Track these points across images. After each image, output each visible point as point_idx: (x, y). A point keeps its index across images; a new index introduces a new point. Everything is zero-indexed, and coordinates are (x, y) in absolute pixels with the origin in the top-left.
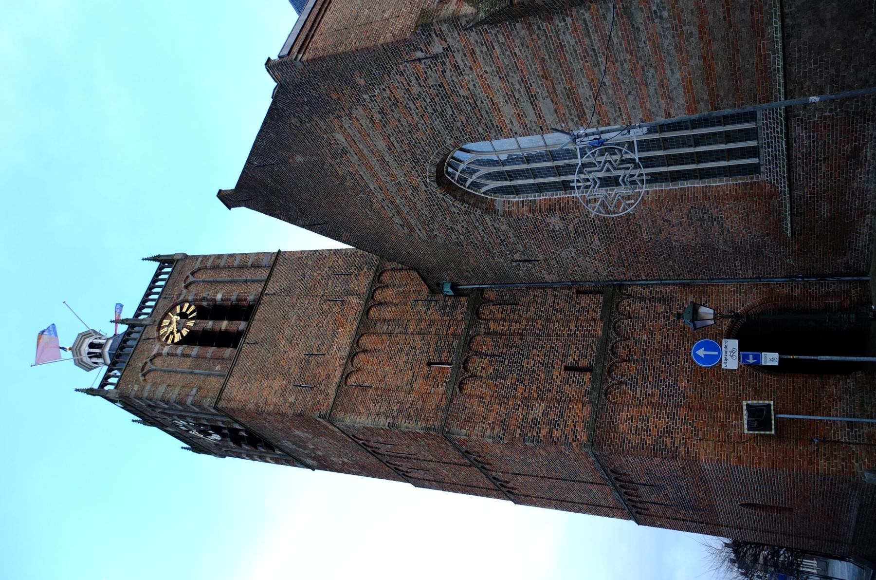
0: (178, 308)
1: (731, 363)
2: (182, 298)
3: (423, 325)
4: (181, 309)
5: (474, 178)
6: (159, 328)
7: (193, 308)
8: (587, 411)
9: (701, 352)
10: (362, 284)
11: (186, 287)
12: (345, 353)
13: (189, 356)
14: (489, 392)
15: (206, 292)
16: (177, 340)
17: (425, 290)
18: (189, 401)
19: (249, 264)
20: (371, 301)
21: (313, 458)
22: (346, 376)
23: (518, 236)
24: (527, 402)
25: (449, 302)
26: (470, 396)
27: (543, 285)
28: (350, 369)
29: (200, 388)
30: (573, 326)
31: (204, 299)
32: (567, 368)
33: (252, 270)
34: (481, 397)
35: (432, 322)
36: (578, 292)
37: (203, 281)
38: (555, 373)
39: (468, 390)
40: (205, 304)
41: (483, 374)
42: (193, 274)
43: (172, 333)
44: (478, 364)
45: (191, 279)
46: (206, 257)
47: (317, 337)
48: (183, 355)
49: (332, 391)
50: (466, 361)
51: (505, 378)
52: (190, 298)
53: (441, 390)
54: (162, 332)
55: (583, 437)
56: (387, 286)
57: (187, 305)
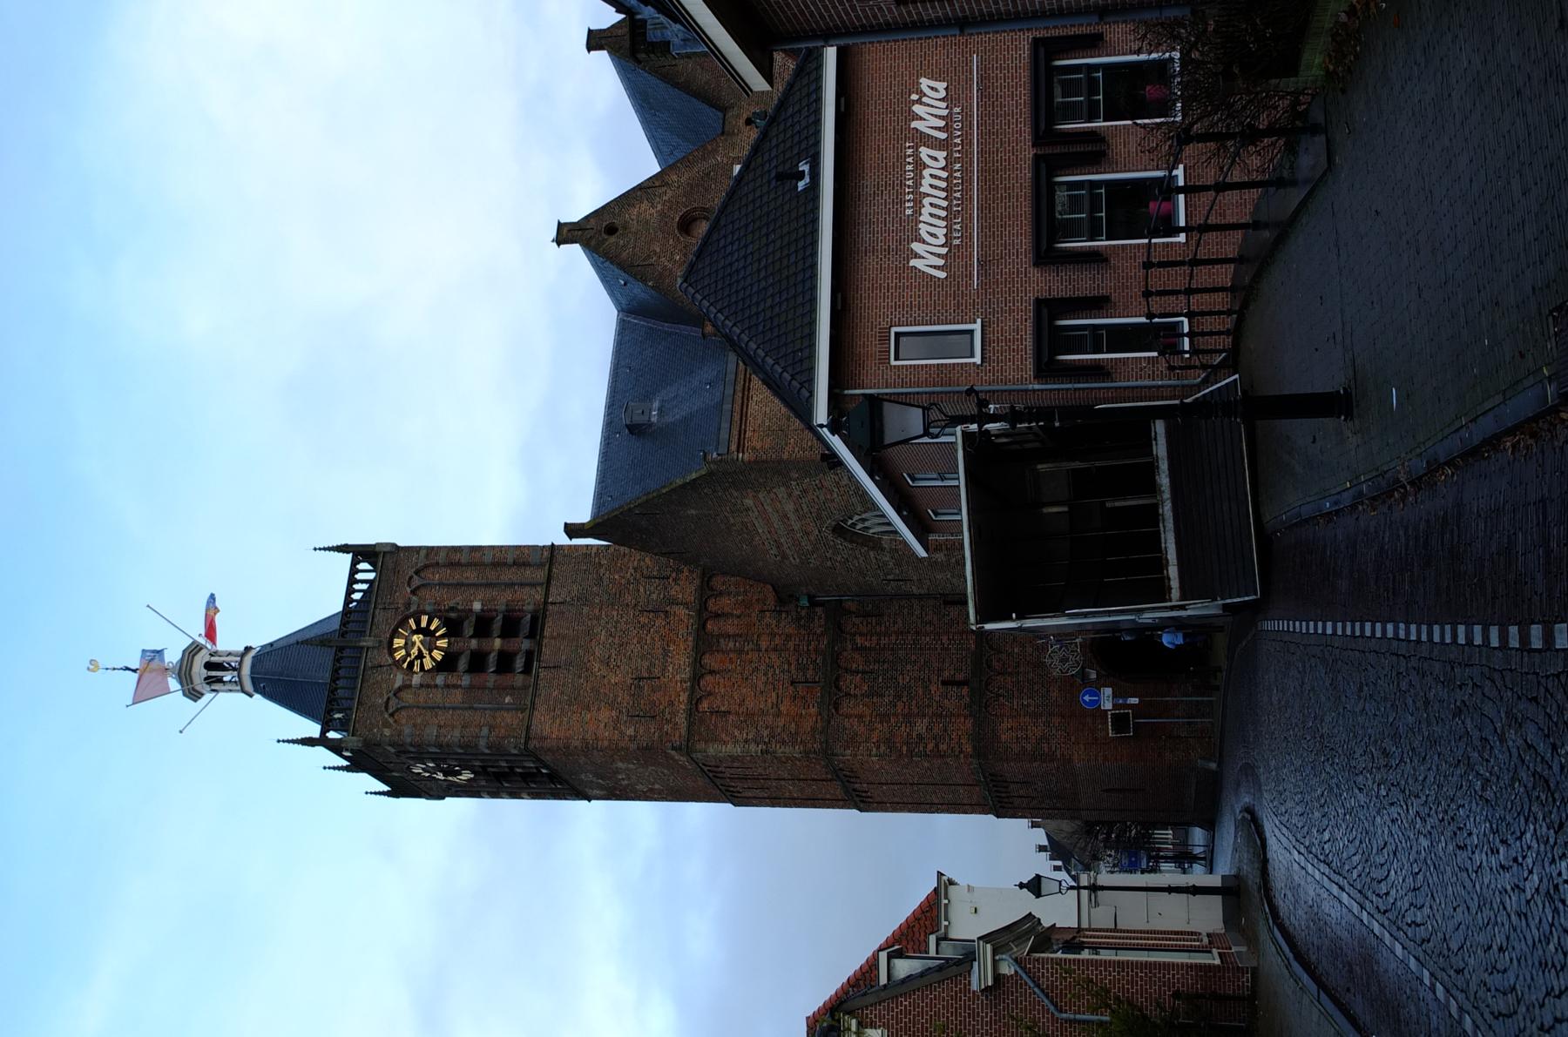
0: (412, 621)
1: (1108, 705)
2: (413, 608)
3: (777, 640)
4: (418, 623)
5: (867, 524)
6: (392, 651)
7: (436, 623)
8: (969, 723)
9: (1087, 698)
10: (685, 588)
11: (413, 592)
12: (686, 673)
13: (456, 687)
14: (868, 712)
15: (457, 600)
16: (428, 664)
17: (771, 601)
18: (482, 743)
19: (510, 560)
20: (703, 613)
21: (601, 787)
22: (694, 702)
23: (898, 564)
24: (909, 718)
25: (803, 613)
26: (848, 716)
27: (909, 596)
28: (698, 694)
29: (491, 728)
30: (945, 639)
31: (452, 609)
32: (944, 683)
33: (513, 569)
34: (860, 717)
35: (789, 637)
36: (947, 603)
37: (441, 584)
38: (933, 688)
39: (844, 709)
40: (453, 615)
41: (858, 692)
42: (417, 573)
43: (420, 656)
44: (851, 682)
45: (416, 582)
46: (431, 550)
47: (643, 657)
48: (447, 686)
49: (681, 719)
50: (837, 679)
51: (882, 696)
52: (428, 608)
53: (813, 710)
54: (398, 655)
55: (968, 748)
56: (721, 594)
57: (424, 619)
